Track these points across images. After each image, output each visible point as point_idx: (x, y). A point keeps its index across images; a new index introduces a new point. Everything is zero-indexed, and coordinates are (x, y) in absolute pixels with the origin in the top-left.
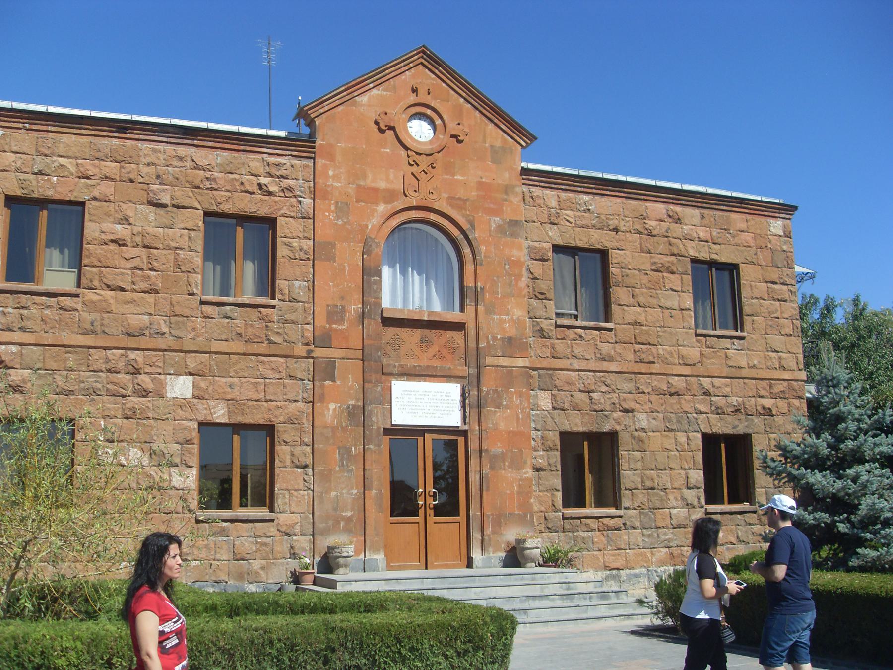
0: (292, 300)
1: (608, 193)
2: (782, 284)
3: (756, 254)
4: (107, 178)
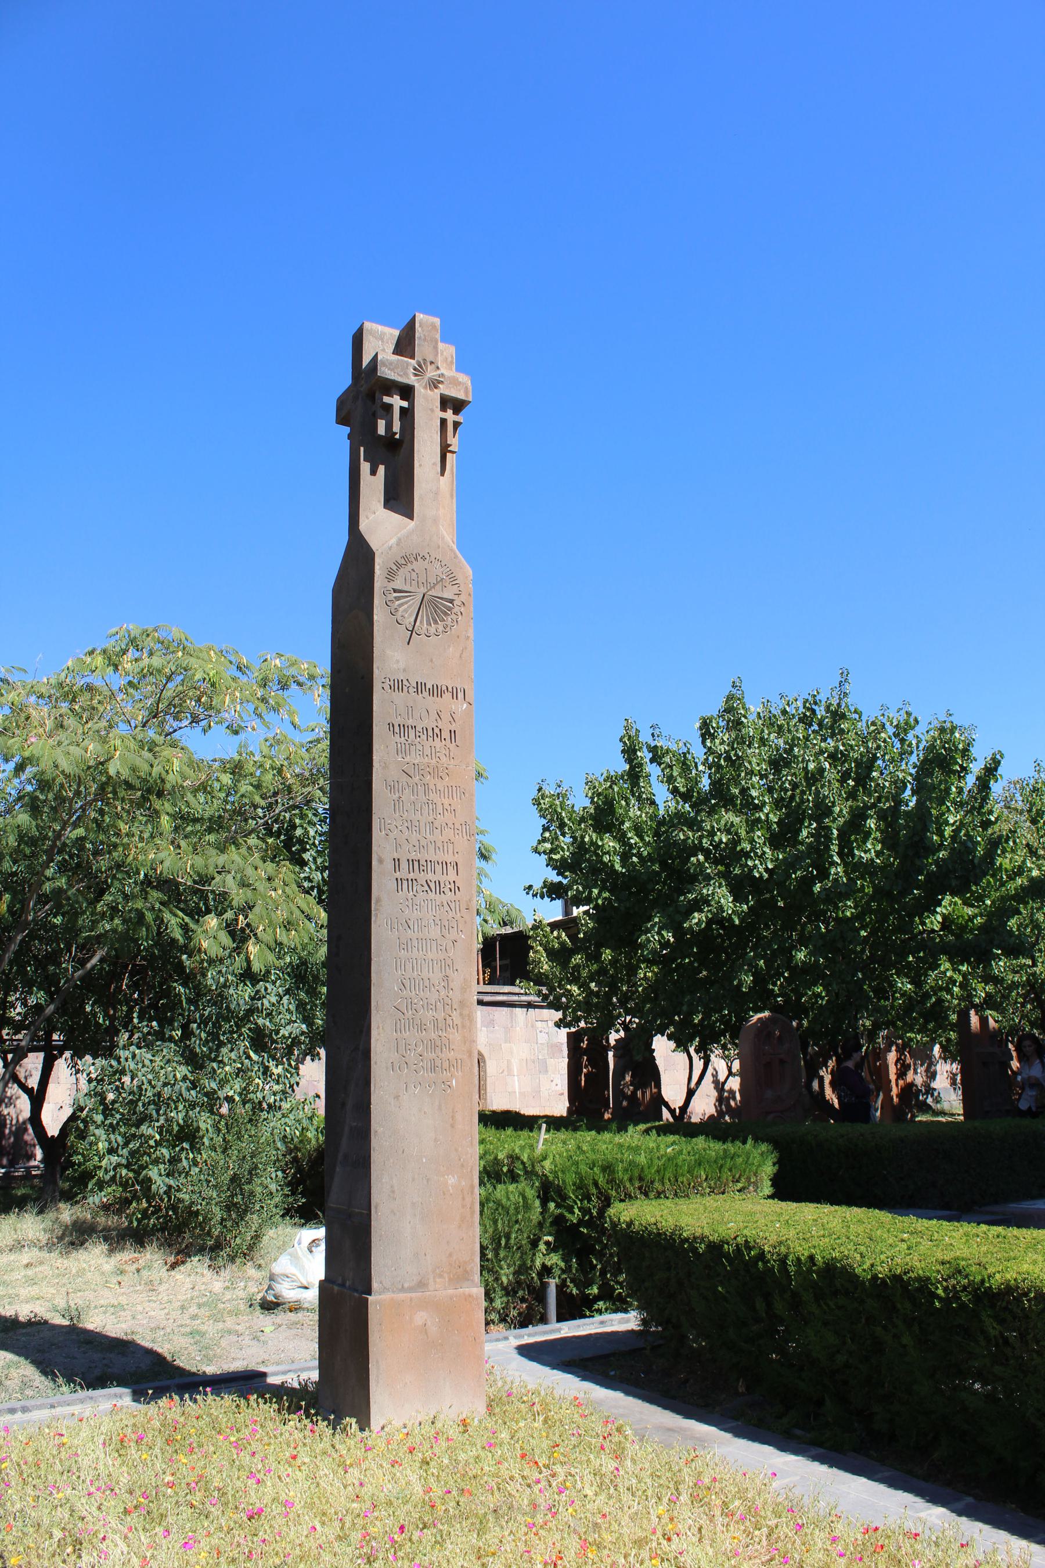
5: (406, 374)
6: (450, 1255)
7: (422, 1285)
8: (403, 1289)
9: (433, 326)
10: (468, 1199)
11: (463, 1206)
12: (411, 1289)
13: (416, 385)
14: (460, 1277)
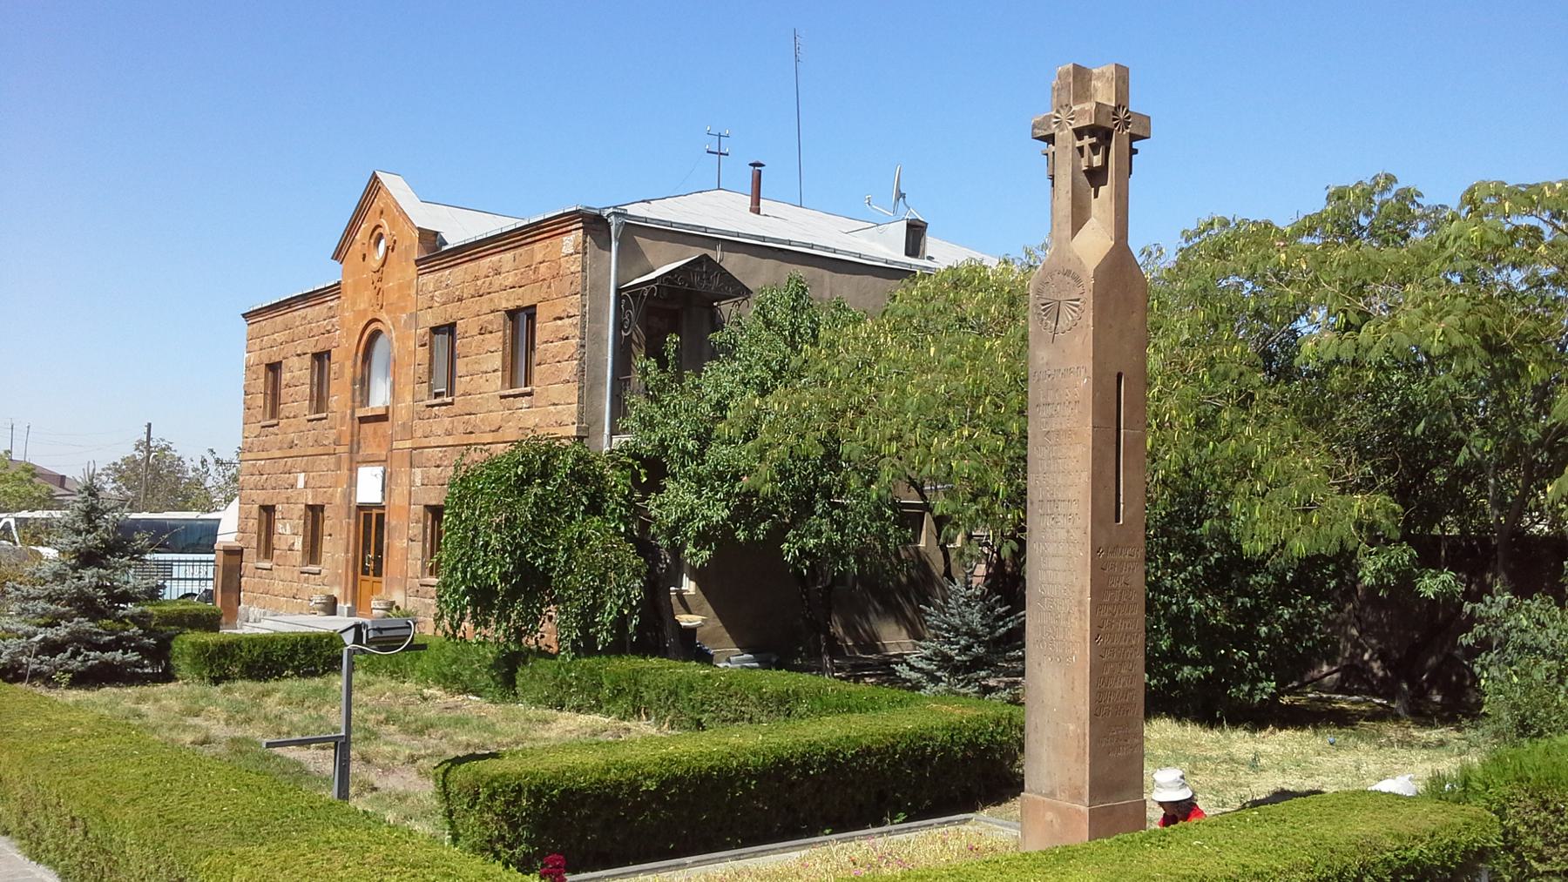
0: (333, 412)
1: (459, 261)
2: (569, 317)
3: (549, 287)
4: (287, 342)
5: (1049, 127)
6: (1070, 779)
7: (1052, 794)
8: (1041, 794)
9: (1068, 72)
10: (1082, 743)
11: (1079, 747)
12: (1046, 795)
13: (1056, 131)
14: (1076, 797)
